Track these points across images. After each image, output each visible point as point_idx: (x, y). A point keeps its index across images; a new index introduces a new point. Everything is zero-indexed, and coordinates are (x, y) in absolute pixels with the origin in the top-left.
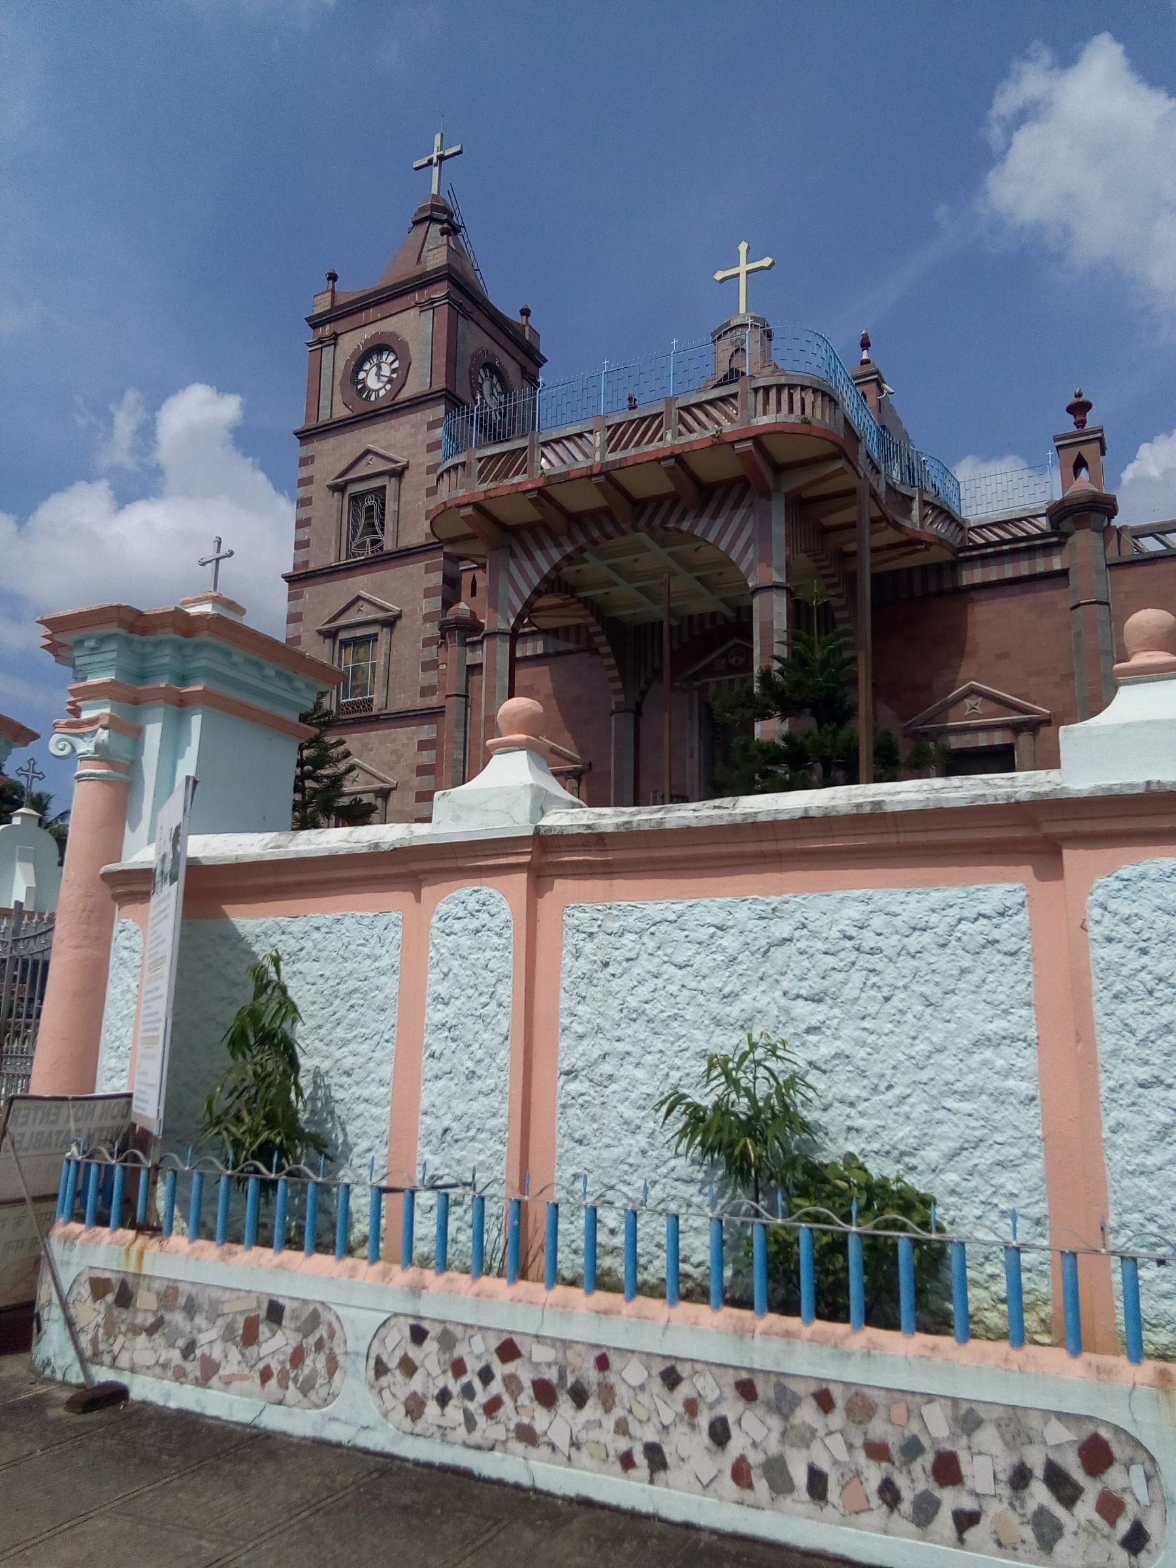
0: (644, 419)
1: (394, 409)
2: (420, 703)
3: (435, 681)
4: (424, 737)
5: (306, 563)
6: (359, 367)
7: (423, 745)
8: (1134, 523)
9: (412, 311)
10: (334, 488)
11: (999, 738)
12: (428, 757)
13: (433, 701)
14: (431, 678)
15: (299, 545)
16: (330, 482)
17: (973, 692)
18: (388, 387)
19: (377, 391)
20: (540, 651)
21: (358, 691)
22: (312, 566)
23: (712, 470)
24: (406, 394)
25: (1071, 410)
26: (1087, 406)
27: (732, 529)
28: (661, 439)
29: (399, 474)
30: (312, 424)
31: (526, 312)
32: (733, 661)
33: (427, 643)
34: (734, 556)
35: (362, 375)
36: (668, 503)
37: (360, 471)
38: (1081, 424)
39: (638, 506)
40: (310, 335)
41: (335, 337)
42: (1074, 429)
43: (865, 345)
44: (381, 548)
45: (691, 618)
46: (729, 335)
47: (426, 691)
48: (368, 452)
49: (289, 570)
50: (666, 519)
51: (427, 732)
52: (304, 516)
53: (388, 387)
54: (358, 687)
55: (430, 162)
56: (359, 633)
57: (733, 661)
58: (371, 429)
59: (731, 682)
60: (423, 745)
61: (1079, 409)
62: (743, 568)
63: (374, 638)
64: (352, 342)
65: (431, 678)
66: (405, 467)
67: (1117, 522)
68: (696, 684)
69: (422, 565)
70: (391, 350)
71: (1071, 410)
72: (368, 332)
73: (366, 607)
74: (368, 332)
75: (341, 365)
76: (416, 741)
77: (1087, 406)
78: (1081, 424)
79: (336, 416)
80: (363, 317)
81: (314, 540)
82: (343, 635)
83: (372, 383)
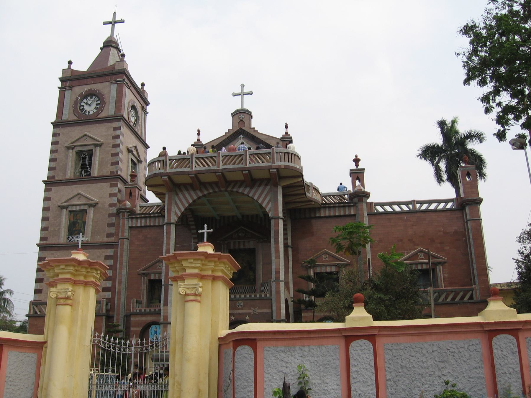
0: (236, 156)
2: (106, 239)
4: (108, 254)
5: (53, 177)
8: (375, 201)
10: (68, 148)
11: (334, 269)
13: (112, 239)
14: (112, 230)
15: (50, 169)
17: (326, 253)
18: (95, 111)
22: (56, 178)
23: (257, 175)
24: (103, 115)
25: (354, 160)
26: (359, 160)
27: (263, 196)
28: (243, 164)
29: (100, 145)
30: (59, 120)
31: (143, 85)
32: (240, 234)
33: (110, 215)
34: (264, 205)
36: (241, 183)
38: (357, 165)
39: (228, 183)
40: (60, 84)
41: (71, 88)
42: (355, 168)
43: (286, 127)
44: (90, 175)
45: (224, 217)
46: (237, 115)
47: (109, 235)
48: (85, 135)
49: (46, 179)
51: (110, 252)
52: (53, 157)
54: (76, 230)
56: (78, 208)
57: (240, 234)
58: (87, 126)
59: (239, 243)
61: (357, 161)
62: (267, 210)
63: (86, 211)
64: (79, 90)
65: (112, 230)
66: (102, 144)
67: (369, 200)
68: (226, 242)
71: (354, 160)
72: (86, 88)
73: (82, 198)
74: (86, 88)
75: (74, 98)
76: (104, 254)
77: (359, 160)
78: (357, 165)
79: (71, 119)
80: (85, 81)
81: (58, 167)
82: (70, 209)
83: (87, 108)
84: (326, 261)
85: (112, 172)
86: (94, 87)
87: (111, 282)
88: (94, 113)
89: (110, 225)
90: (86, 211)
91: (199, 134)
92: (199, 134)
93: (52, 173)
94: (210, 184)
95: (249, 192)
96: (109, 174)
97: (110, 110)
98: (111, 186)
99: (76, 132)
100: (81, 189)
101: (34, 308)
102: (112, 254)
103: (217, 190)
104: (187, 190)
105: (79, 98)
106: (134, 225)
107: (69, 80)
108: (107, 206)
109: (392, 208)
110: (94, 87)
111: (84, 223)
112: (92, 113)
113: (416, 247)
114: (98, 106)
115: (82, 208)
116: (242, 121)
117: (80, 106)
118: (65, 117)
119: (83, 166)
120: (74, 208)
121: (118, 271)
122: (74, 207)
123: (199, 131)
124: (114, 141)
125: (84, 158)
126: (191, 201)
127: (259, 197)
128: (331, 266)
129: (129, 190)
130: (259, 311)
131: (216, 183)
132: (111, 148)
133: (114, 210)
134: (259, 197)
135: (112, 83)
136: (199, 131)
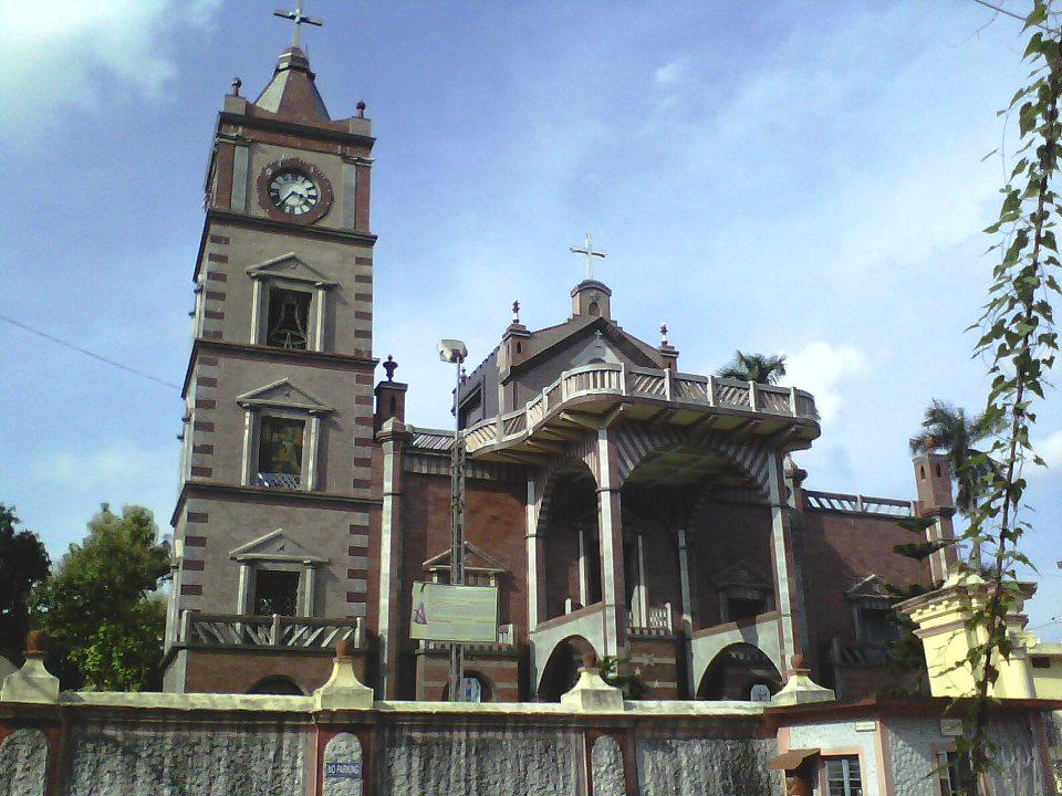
1: (306, 228)
2: (353, 492)
5: (219, 334)
6: (273, 178)
7: (355, 529)
9: (333, 157)
13: (367, 493)
16: (252, 267)
19: (293, 208)
22: (226, 339)
33: (360, 442)
35: (274, 186)
43: (664, 331)
47: (358, 483)
48: (292, 259)
51: (360, 518)
53: (306, 209)
54: (280, 463)
60: (355, 529)
66: (335, 285)
70: (308, 177)
74: (285, 154)
80: (281, 138)
86: (308, 157)
88: (304, 214)
90: (302, 424)
91: (516, 310)
92: (516, 310)
93: (214, 325)
96: (351, 353)
97: (338, 219)
99: (275, 248)
100: (281, 373)
101: (202, 628)
104: (638, 435)
105: (269, 172)
107: (243, 124)
110: (308, 157)
111: (298, 450)
112: (298, 211)
114: (313, 202)
116: (594, 306)
117: (273, 190)
118: (238, 205)
120: (275, 414)
123: (516, 304)
126: (644, 454)
127: (751, 466)
130: (657, 660)
131: (685, 430)
134: (751, 466)
135: (346, 158)
136: (516, 304)
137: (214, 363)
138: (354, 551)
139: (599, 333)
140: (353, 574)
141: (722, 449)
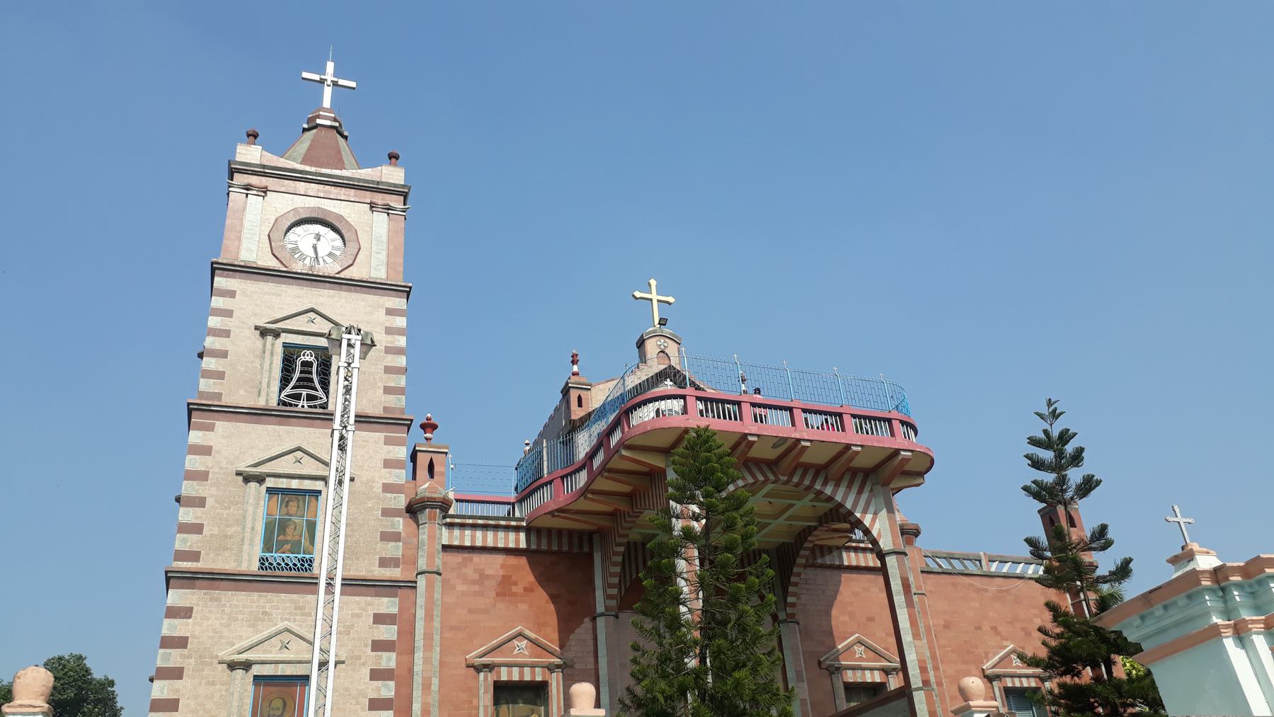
3: (399, 554)
4: (383, 610)
5: (219, 396)
7: (379, 619)
10: (264, 332)
12: (388, 632)
13: (395, 573)
20: (523, 545)
21: (287, 547)
22: (226, 400)
36: (821, 470)
37: (300, 323)
41: (265, 191)
44: (324, 406)
47: (384, 563)
48: (312, 310)
50: (813, 481)
51: (387, 605)
54: (287, 542)
55: (322, 81)
56: (295, 484)
60: (379, 619)
69: (382, 435)
72: (300, 202)
76: (371, 613)
80: (301, 187)
82: (270, 482)
84: (861, 659)
85: (386, 409)
87: (392, 684)
89: (387, 537)
94: (760, 463)
95: (835, 491)
96: (378, 412)
98: (388, 442)
102: (395, 610)
103: (772, 477)
106: (456, 543)
108: (378, 488)
109: (951, 564)
111: (312, 526)
113: (1005, 643)
115: (308, 485)
119: (305, 382)
120: (283, 483)
121: (419, 656)
122: (285, 480)
124: (390, 338)
125: (307, 364)
128: (871, 669)
129: (428, 456)
131: (772, 464)
132: (383, 354)
133: (401, 501)
137: (211, 428)
138: (378, 646)
139: (668, 382)
140: (376, 675)
141: (818, 487)
